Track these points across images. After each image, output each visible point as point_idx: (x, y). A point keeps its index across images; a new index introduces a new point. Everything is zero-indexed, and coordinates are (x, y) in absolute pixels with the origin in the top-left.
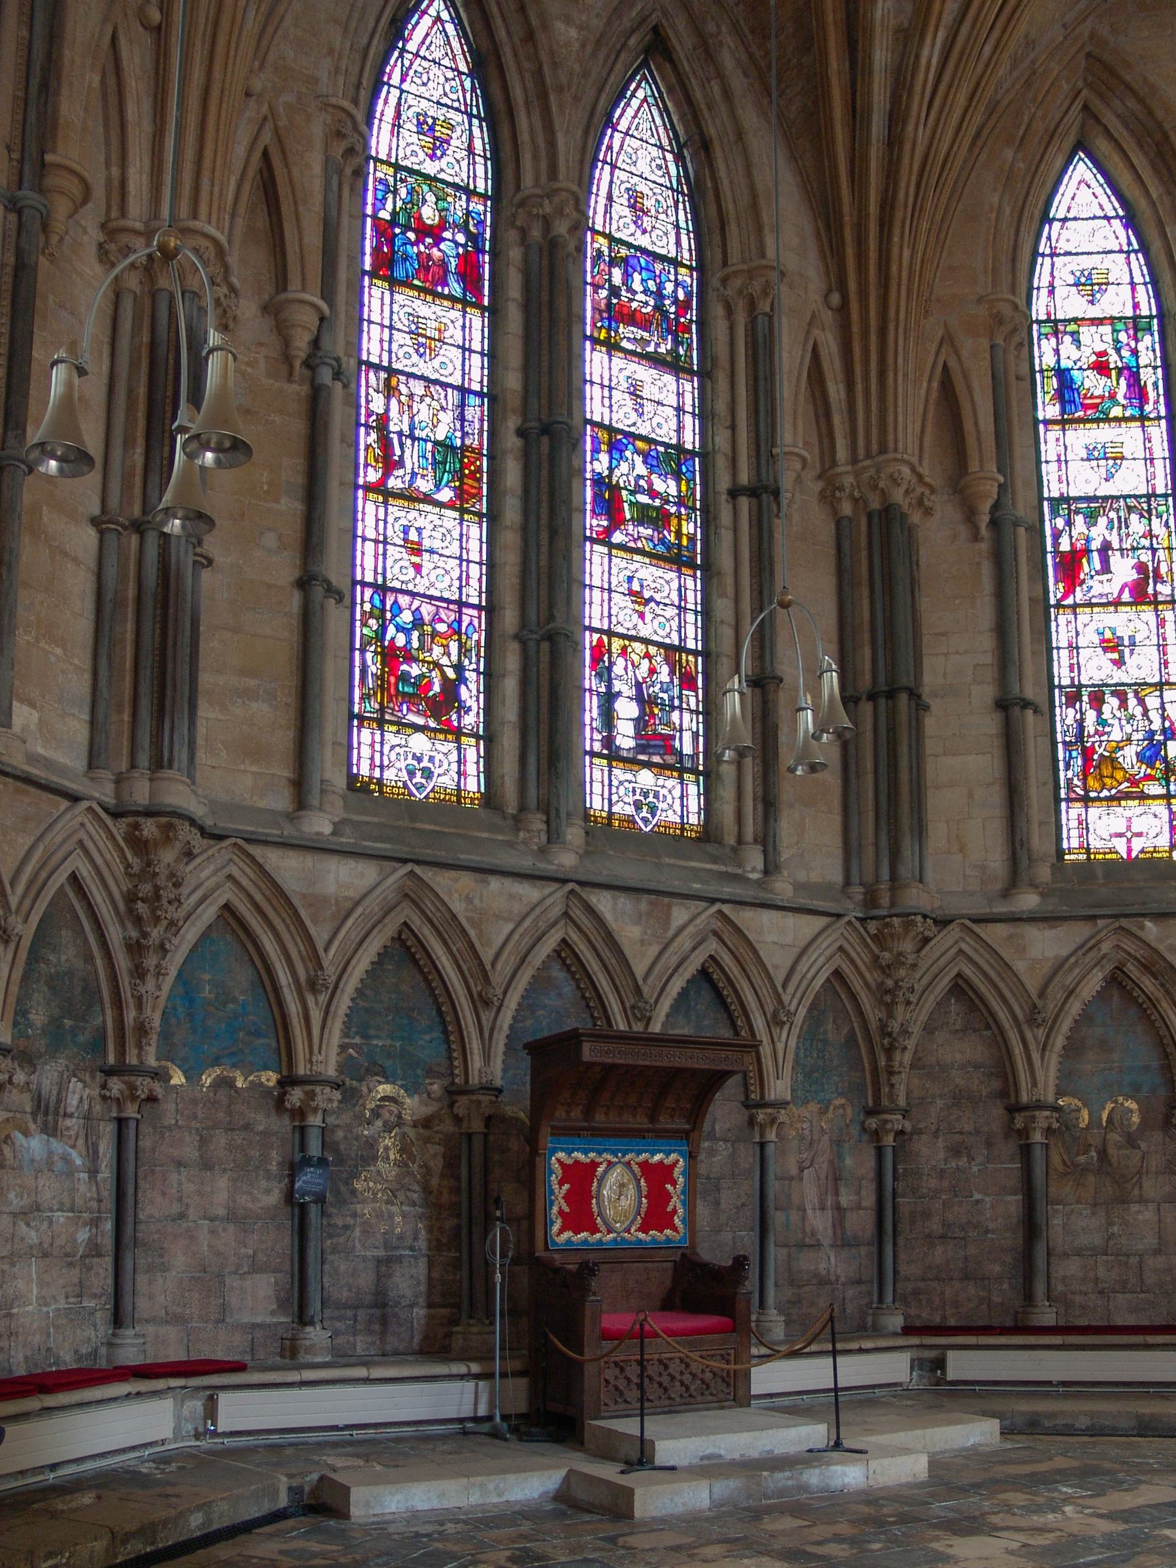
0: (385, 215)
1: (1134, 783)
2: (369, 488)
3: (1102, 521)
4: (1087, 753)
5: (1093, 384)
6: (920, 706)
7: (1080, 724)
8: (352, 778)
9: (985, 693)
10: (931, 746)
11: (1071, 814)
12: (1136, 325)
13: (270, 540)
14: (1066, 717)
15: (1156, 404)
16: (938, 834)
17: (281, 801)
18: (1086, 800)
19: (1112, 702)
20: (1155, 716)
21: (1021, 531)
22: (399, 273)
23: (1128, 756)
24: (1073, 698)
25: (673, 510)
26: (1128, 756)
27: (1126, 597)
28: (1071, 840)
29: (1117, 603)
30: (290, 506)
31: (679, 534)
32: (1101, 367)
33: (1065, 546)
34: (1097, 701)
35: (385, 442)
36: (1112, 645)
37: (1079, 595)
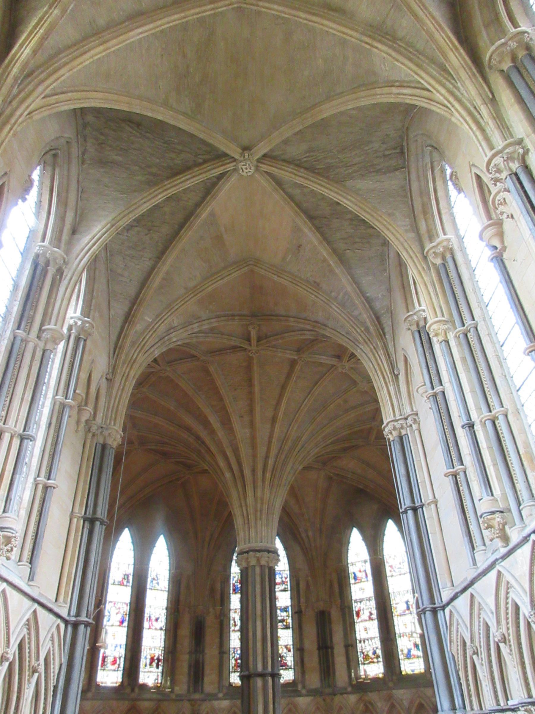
0: (234, 582)
1: (372, 659)
2: (233, 631)
3: (362, 603)
4: (363, 653)
5: (359, 575)
6: (332, 648)
7: (362, 646)
8: (230, 683)
9: (342, 644)
10: (335, 656)
11: (362, 667)
12: (365, 562)
13: (215, 647)
14: (359, 645)
15: (370, 577)
16: (337, 674)
17: (216, 691)
18: (364, 664)
19: (366, 641)
20: (374, 644)
21: (346, 609)
22: (236, 591)
23: (370, 654)
24: (360, 642)
25: (285, 618)
26: (370, 654)
27: (368, 618)
28: (362, 673)
29: (366, 621)
30: (217, 640)
31: (287, 623)
32: (360, 571)
33: (357, 610)
34: (364, 642)
35: (235, 622)
36: (366, 630)
37: (360, 619)
